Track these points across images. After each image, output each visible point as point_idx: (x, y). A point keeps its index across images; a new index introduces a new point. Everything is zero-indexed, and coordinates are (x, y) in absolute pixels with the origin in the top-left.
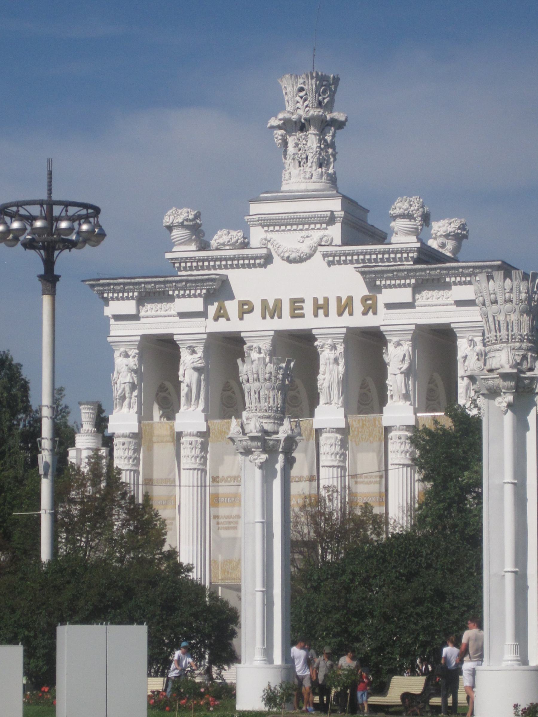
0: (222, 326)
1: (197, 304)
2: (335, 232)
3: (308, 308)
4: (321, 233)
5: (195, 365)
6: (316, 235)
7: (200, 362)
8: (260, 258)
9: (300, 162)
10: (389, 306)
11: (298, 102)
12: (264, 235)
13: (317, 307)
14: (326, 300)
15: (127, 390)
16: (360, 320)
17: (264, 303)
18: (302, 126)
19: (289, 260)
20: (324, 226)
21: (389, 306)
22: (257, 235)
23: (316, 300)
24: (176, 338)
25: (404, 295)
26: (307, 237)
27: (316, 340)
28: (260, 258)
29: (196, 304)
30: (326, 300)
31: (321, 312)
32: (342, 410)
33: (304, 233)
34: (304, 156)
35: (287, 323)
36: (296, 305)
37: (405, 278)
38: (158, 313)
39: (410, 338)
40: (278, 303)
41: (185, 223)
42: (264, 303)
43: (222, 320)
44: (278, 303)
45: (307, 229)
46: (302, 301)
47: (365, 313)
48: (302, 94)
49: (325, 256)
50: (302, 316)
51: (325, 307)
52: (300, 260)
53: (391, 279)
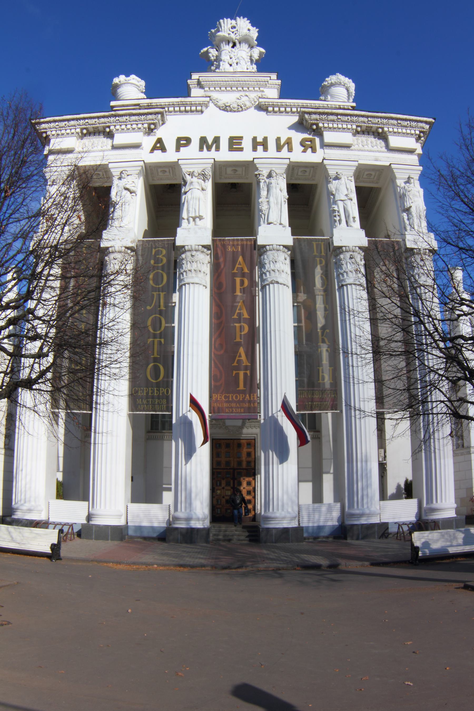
3: (247, 144)
5: (128, 186)
6: (253, 95)
7: (133, 185)
13: (255, 144)
14: (265, 139)
16: (299, 156)
17: (203, 141)
23: (254, 139)
24: (110, 166)
26: (247, 96)
30: (265, 139)
31: (260, 148)
32: (289, 229)
33: (243, 94)
36: (235, 143)
39: (352, 173)
40: (217, 140)
42: (203, 141)
43: (158, 153)
44: (217, 140)
45: (245, 91)
46: (241, 138)
47: (304, 151)
50: (241, 150)
51: (264, 144)
52: (241, 109)
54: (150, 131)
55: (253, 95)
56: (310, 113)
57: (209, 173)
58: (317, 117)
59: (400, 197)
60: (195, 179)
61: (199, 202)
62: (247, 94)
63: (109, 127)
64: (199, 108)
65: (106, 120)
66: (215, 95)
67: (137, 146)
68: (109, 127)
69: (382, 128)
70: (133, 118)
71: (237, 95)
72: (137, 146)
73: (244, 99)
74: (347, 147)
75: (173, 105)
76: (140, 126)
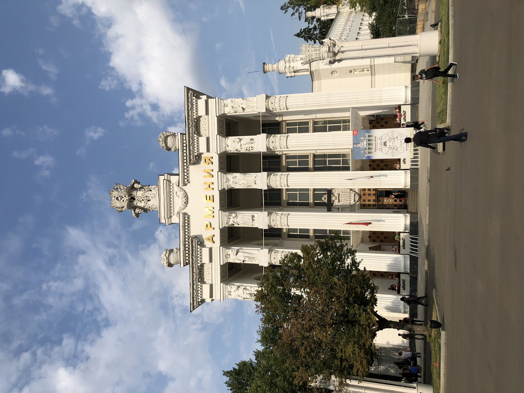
0: (217, 239)
1: (205, 252)
2: (174, 179)
3: (210, 193)
4: (175, 186)
5: (235, 254)
8: (184, 218)
9: (149, 200)
10: (208, 150)
11: (123, 201)
12: (175, 216)
15: (247, 292)
18: (132, 199)
19: (186, 203)
20: (171, 184)
21: (208, 150)
22: (175, 219)
25: (202, 141)
27: (224, 189)
28: (184, 218)
29: (205, 252)
33: (175, 195)
34: (146, 198)
35: (217, 203)
37: (193, 140)
38: (210, 273)
41: (167, 256)
48: (120, 199)
49: (185, 185)
52: (186, 196)
53: (193, 147)
54: (202, 244)
55: (176, 189)
56: (190, 160)
57: (227, 213)
58: (191, 156)
59: (236, 112)
60: (231, 220)
61: (243, 219)
62: (175, 193)
63: (198, 266)
64: (186, 219)
65: (194, 269)
66: (176, 210)
67: (211, 250)
68: (198, 266)
69: (194, 119)
70: (194, 254)
71: (176, 198)
72: (211, 250)
73: (179, 193)
74: (208, 139)
75: (185, 232)
76: (199, 250)
